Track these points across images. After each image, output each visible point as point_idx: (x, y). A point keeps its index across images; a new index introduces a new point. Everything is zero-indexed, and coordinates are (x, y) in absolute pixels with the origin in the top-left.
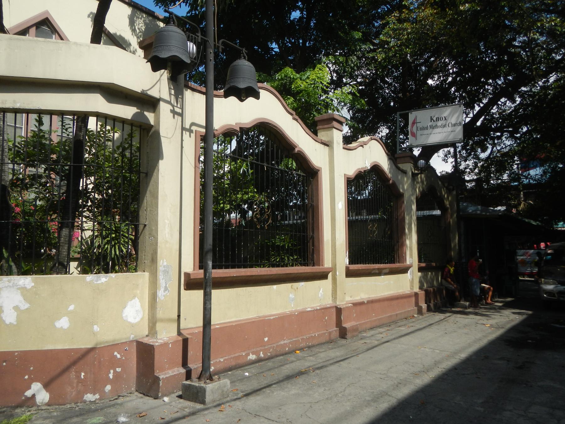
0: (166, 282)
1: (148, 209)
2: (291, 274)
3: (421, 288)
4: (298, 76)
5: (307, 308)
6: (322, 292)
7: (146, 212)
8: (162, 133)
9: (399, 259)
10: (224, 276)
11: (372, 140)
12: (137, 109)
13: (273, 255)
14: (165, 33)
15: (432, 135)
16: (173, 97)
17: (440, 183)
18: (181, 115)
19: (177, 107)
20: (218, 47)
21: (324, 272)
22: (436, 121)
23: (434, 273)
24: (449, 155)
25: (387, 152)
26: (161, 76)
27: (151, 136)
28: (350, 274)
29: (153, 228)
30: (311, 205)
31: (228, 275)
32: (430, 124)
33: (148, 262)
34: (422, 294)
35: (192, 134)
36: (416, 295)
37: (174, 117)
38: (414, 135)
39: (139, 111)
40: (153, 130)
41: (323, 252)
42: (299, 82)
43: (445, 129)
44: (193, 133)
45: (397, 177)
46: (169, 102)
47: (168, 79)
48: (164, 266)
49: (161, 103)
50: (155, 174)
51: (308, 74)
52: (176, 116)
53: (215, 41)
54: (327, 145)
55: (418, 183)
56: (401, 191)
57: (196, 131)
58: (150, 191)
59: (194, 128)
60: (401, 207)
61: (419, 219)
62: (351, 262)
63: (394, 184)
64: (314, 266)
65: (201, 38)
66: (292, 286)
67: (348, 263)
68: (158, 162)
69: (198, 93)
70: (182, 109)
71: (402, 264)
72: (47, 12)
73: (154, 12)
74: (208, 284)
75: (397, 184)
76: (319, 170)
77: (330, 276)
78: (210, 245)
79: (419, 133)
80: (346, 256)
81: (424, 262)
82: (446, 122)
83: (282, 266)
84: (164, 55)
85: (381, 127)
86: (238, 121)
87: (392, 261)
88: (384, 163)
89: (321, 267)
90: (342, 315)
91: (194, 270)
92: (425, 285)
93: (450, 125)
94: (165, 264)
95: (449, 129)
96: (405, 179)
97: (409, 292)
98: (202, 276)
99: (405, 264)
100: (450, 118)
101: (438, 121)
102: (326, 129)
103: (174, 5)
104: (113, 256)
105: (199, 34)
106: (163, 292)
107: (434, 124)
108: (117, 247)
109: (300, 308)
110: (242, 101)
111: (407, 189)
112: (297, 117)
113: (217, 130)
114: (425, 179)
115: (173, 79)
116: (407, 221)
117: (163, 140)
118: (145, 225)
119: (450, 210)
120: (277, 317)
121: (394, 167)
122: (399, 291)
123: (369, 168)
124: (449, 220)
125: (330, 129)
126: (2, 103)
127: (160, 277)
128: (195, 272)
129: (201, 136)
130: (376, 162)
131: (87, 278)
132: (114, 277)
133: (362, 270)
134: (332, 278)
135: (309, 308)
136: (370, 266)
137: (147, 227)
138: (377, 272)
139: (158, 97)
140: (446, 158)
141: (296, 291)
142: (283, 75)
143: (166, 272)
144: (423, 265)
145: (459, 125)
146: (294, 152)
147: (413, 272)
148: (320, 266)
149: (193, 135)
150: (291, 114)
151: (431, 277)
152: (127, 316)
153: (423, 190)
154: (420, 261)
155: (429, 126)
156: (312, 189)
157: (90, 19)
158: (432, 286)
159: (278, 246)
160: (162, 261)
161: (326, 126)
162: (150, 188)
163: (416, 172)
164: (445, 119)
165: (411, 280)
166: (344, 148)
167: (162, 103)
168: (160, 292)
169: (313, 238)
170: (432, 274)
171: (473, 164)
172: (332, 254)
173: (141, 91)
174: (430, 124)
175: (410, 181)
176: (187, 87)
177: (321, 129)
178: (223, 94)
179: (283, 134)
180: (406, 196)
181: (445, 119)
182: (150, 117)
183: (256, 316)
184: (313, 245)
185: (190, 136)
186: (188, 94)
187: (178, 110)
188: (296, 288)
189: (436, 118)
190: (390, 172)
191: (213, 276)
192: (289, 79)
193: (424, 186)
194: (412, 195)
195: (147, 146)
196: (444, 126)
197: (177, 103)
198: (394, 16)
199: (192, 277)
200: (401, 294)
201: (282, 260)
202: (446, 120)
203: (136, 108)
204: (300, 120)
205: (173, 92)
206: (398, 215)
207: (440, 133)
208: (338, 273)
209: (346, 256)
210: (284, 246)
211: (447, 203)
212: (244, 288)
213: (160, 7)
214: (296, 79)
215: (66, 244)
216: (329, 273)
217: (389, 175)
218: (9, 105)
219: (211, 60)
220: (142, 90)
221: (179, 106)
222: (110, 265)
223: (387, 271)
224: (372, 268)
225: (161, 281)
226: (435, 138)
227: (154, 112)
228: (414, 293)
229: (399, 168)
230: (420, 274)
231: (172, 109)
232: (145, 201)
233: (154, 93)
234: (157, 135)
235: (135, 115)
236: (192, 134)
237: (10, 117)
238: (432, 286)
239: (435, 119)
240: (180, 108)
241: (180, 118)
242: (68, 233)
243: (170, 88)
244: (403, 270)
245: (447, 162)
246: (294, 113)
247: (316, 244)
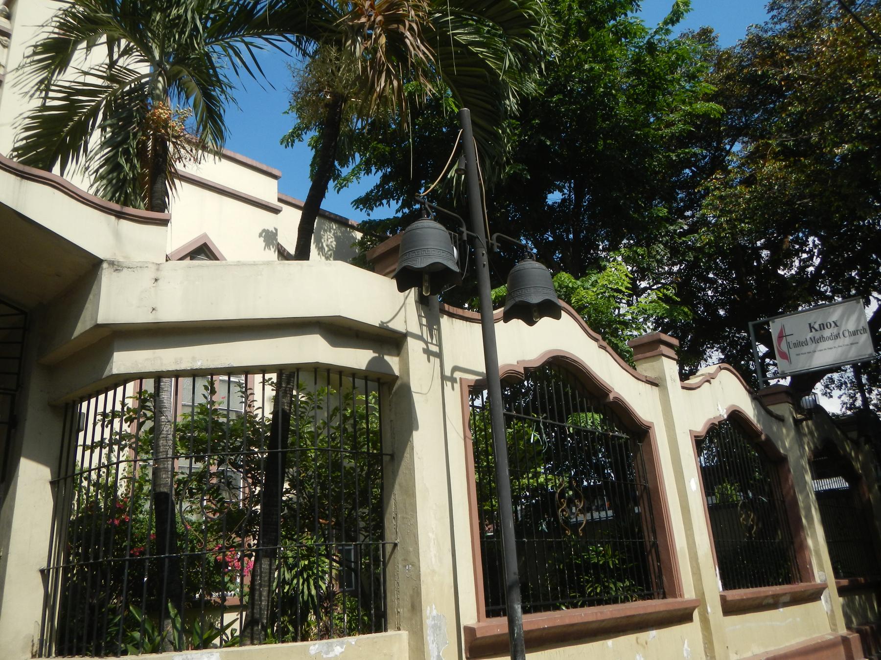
0: (438, 648)
1: (399, 516)
2: (633, 616)
3: (849, 627)
4: (579, 283)
7: (396, 521)
8: (414, 387)
9: (799, 573)
11: (721, 369)
12: (374, 352)
13: (588, 581)
14: (418, 231)
15: (817, 354)
16: (425, 328)
17: (839, 432)
18: (439, 355)
19: (432, 343)
20: (492, 244)
21: (686, 609)
22: (821, 329)
23: (863, 597)
24: (833, 386)
25: (748, 387)
26: (406, 298)
27: (395, 392)
28: (730, 609)
29: (411, 549)
30: (645, 487)
32: (810, 335)
33: (404, 611)
34: (854, 637)
35: (455, 385)
36: (845, 640)
37: (429, 360)
38: (784, 356)
39: (377, 355)
40: (399, 383)
41: (677, 571)
42: (583, 293)
43: (841, 341)
44: (456, 382)
45: (771, 428)
46: (420, 338)
47: (416, 302)
48: (434, 618)
49: (409, 339)
50: (407, 455)
51: (593, 278)
52: (432, 358)
53: (487, 237)
54: (656, 385)
55: (805, 435)
56: (782, 451)
57: (461, 379)
58: (400, 485)
59: (458, 375)
60: (787, 480)
61: (821, 496)
62: (726, 586)
63: (768, 439)
64: (664, 597)
65: (468, 234)
66: (637, 639)
67: (721, 589)
68: (410, 434)
69: (458, 321)
70: (440, 345)
71: (808, 584)
72: (205, 236)
73: (347, 220)
74: (519, 649)
75: (774, 440)
76: (649, 427)
77: (696, 615)
78: (515, 574)
79: (793, 352)
81: (845, 577)
82: (839, 330)
83: (607, 602)
84: (421, 263)
85: (708, 350)
86: (520, 359)
87: (788, 581)
88: (748, 408)
89: (679, 599)
91: (479, 621)
92: (854, 620)
93: (847, 334)
94: (435, 613)
95: (847, 340)
96: (784, 431)
97: (831, 637)
98: (506, 630)
99: (813, 583)
100: (844, 323)
101: (824, 329)
103: (380, 205)
104: (305, 598)
105: (464, 229)
107: (817, 335)
108: (312, 582)
110: (531, 322)
111: (791, 447)
112: (605, 344)
114: (813, 428)
115: (423, 302)
116: (801, 504)
117: (416, 398)
118: (395, 545)
119: (864, 478)
121: (763, 412)
122: (814, 636)
123: (725, 417)
124: (867, 495)
126: (176, 362)
127: (428, 638)
128: (482, 624)
130: (734, 406)
131: (312, 648)
132: (353, 643)
133: (748, 599)
134: (700, 619)
136: (759, 592)
137: (399, 548)
138: (771, 601)
139: (404, 331)
140: (829, 391)
141: (644, 648)
142: (556, 284)
143: (437, 628)
144: (845, 582)
145: (862, 332)
147: (830, 597)
148: (676, 597)
149: (457, 386)
150: (596, 340)
151: (860, 604)
153: (816, 447)
154: (837, 575)
155: (808, 339)
156: (642, 461)
157: (262, 239)
158: (867, 622)
159: (596, 565)
160: (429, 608)
161: (648, 354)
162: (401, 478)
163: (799, 416)
164: (836, 325)
165: (829, 613)
166: (683, 388)
167: (410, 340)
169: (655, 545)
170: (860, 598)
171: (879, 397)
172: (693, 574)
174: (810, 335)
175: (793, 433)
176: (444, 312)
178: (502, 315)
179: (589, 373)
180: (791, 460)
181: (836, 325)
182: (393, 362)
184: (659, 560)
185: (453, 388)
186: (445, 320)
187: (434, 348)
188: (644, 643)
189: (820, 325)
190: (758, 421)
191: (526, 628)
192: (564, 290)
193: (815, 440)
194: (802, 456)
195: (390, 410)
196: (837, 336)
197: (432, 338)
198: (716, 178)
199: (479, 635)
200: (819, 641)
201: (607, 590)
202: (837, 326)
204: (609, 349)
205: (424, 321)
206: (784, 493)
207: (831, 348)
210: (606, 563)
211: (857, 466)
212: (561, 650)
213: (361, 210)
214: (578, 288)
216: (694, 609)
217: (759, 427)
218: (185, 365)
219: (484, 265)
221: (434, 342)
223: (787, 599)
224: (762, 595)
225: (431, 645)
226: (823, 357)
227: (398, 354)
228: (840, 638)
229: (770, 413)
230: (841, 600)
231: (425, 347)
232: (392, 502)
233: (398, 325)
234: (406, 392)
235: (372, 362)
237: (185, 383)
238: (867, 622)
239: (817, 326)
240: (436, 345)
241: (438, 361)
242: (268, 567)
243: (419, 316)
244: (813, 594)
245: (831, 397)
246: (599, 337)
247: (663, 556)
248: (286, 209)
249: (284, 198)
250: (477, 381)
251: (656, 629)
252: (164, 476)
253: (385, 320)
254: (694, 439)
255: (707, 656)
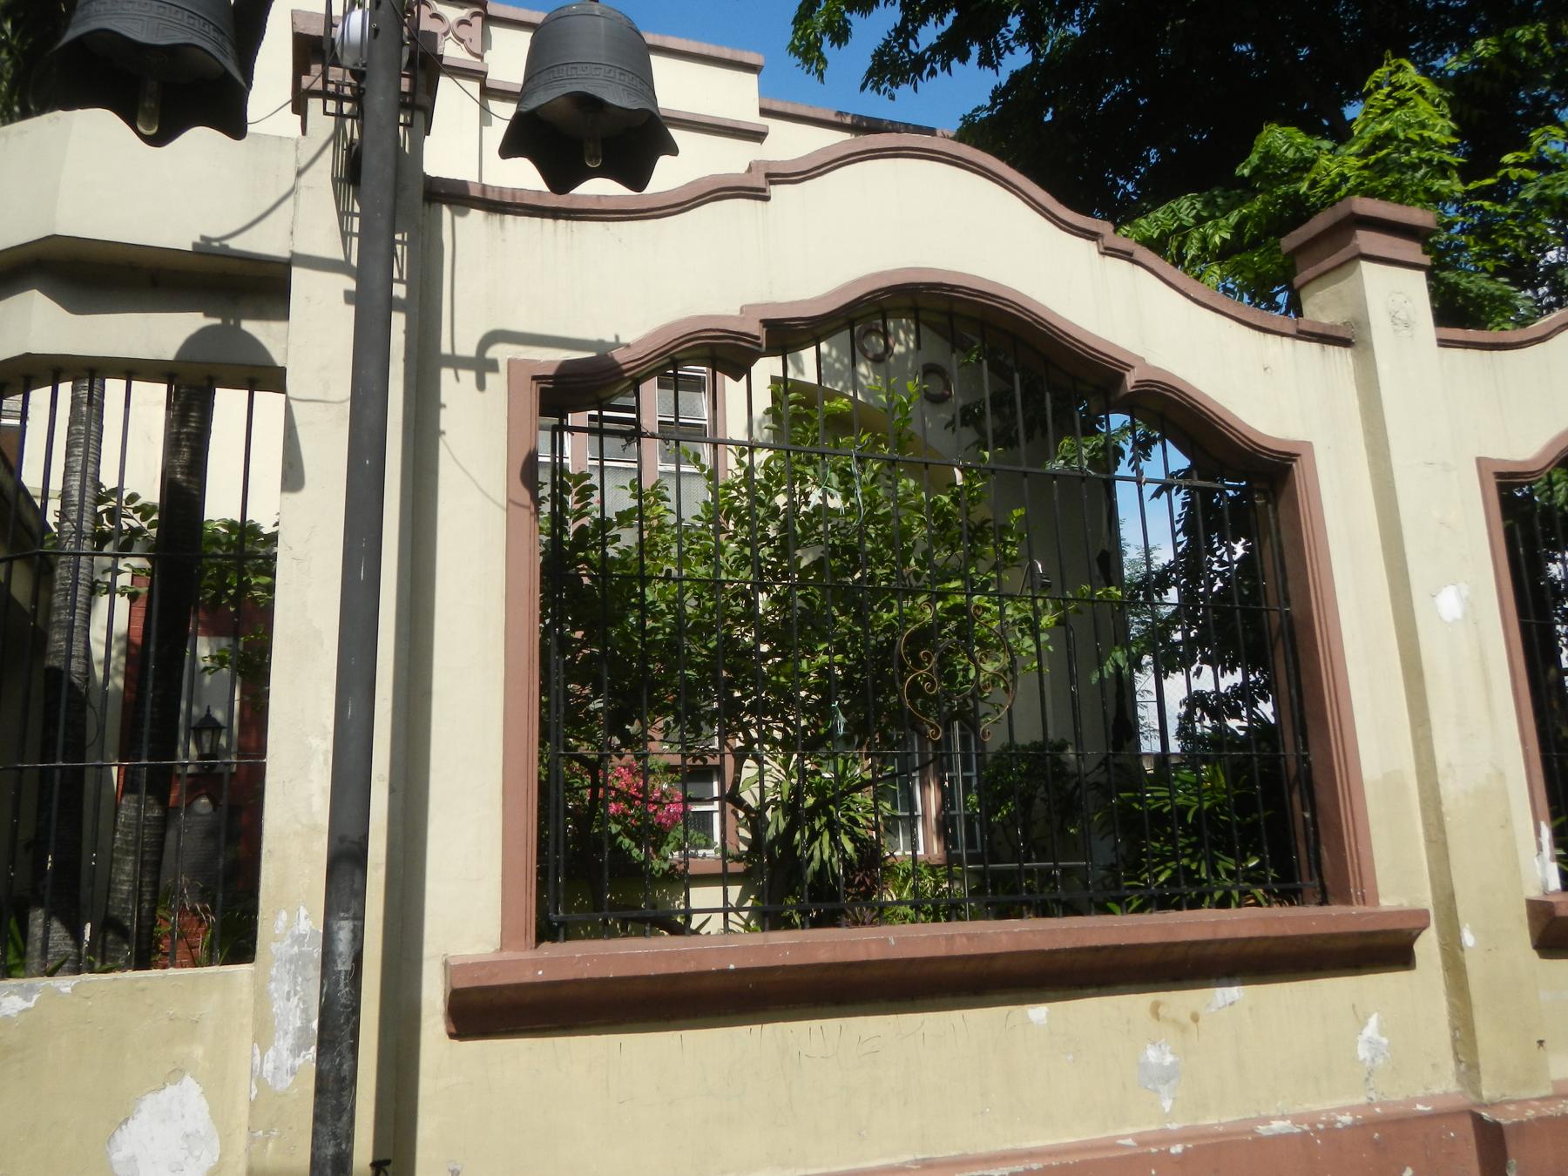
5: (1266, 1120)
6: (1382, 1032)
10: (662, 968)
12: (207, 315)
31: (691, 967)
35: (490, 378)
47: (335, 181)
54: (1345, 342)
57: (510, 362)
59: (498, 352)
64: (1324, 901)
76: (1292, 457)
77: (1427, 947)
80: (1540, 848)
86: (753, 298)
89: (1356, 909)
90: (1513, 1162)
102: (1332, 276)
106: (285, 1054)
109: (1214, 1119)
113: (628, 346)
120: (1035, 1166)
125: (1348, 268)
128: (508, 955)
129: (534, 378)
132: (68, 990)
134: (1445, 963)
135: (1283, 1117)
141: (1184, 1029)
146: (1122, 393)
149: (497, 382)
152: (132, 1159)
160: (284, 915)
166: (1443, 343)
167: (299, 276)
168: (271, 1053)
172: (1430, 842)
173: (195, 245)
177: (1308, 282)
183: (908, 1157)
184: (1311, 801)
185: (481, 385)
188: (1185, 1018)
203: (200, 315)
208: (1468, 939)
209: (1540, 848)
215: (127, 853)
220: (203, 238)
222: (87, 937)
233: (266, 242)
236: (490, 378)
243: (343, 215)
247: (1322, 797)
248: (773, 125)
249: (767, 106)
250: (566, 365)
251: (1243, 984)
252: (57, 637)
253: (214, 232)
254: (1492, 484)
255: (1459, 1062)
